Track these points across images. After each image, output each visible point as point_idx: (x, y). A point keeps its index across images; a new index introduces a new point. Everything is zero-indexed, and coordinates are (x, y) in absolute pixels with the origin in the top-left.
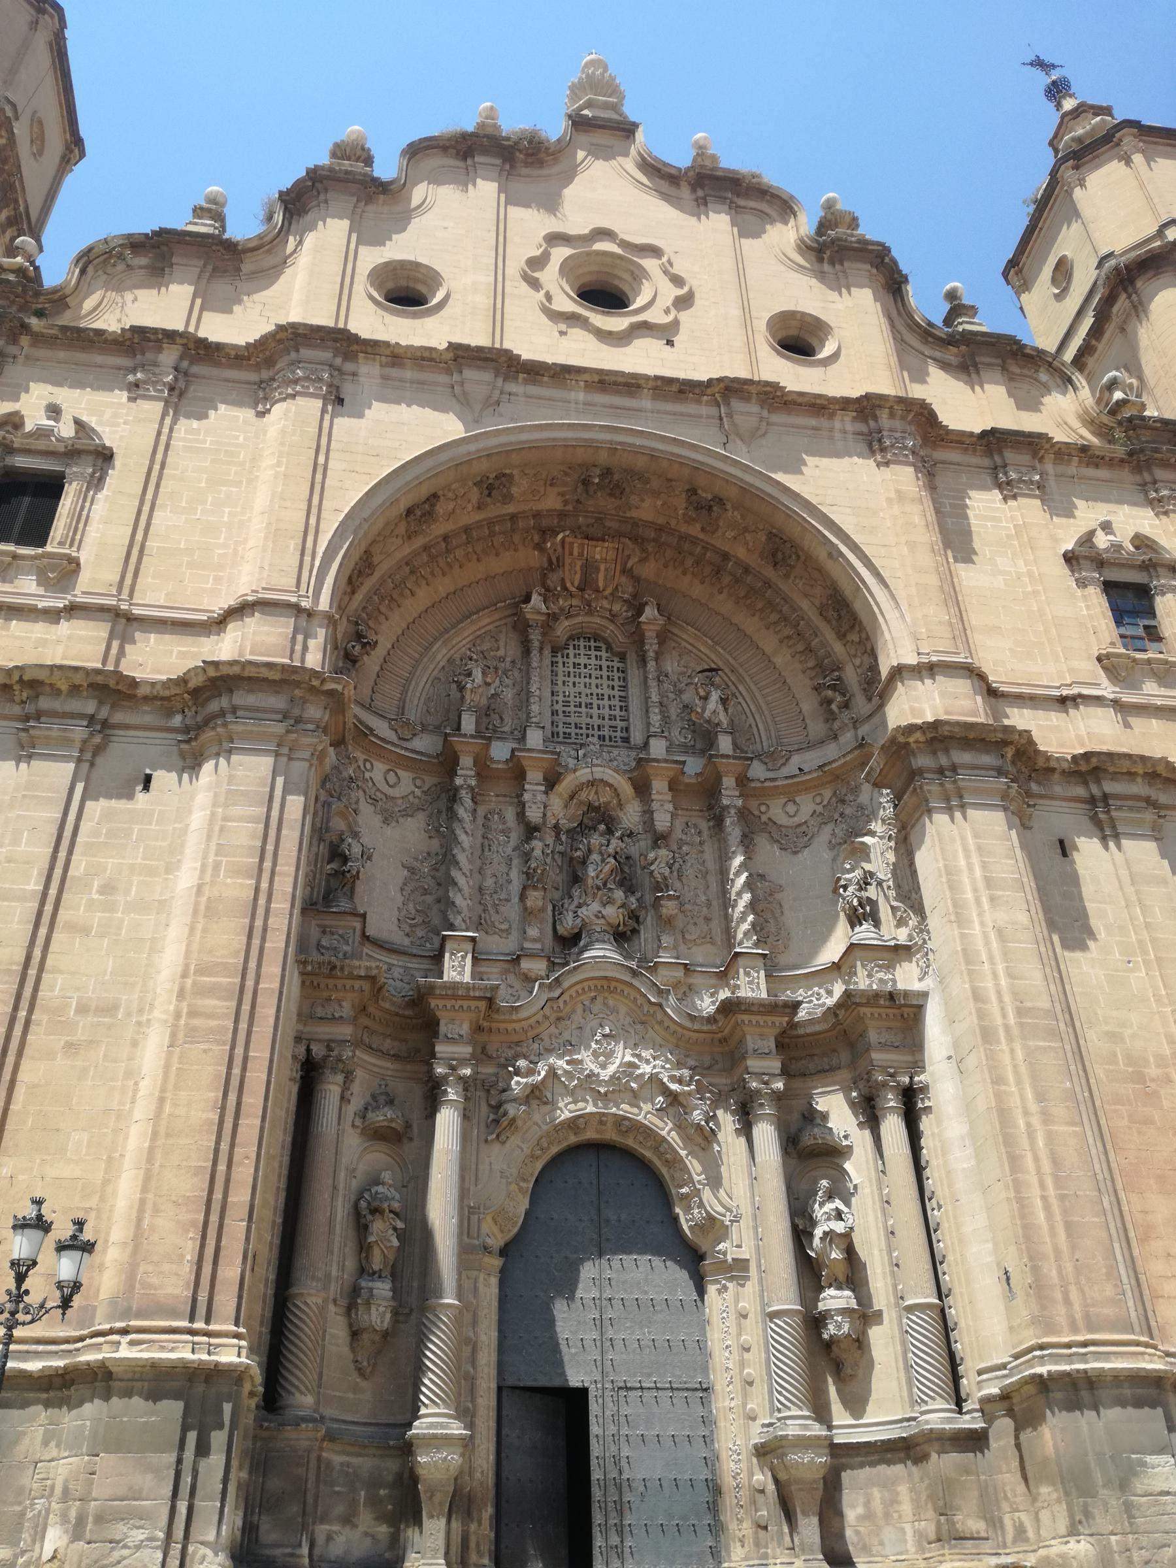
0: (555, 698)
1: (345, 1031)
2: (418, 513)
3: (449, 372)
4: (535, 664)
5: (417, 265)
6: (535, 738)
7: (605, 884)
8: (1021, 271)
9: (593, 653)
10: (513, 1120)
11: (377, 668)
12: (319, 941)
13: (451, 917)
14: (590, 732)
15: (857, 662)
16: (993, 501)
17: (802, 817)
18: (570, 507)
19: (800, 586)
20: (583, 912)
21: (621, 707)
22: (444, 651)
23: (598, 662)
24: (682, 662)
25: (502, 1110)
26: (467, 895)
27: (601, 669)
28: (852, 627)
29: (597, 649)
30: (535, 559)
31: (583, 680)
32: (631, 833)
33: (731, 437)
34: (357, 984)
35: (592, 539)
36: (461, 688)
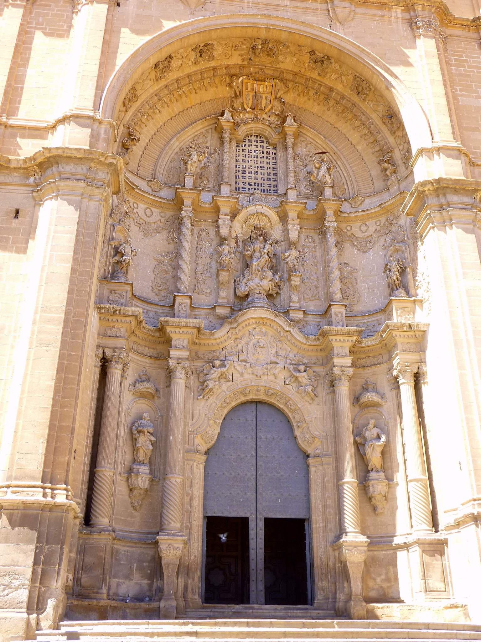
0: (238, 169)
1: (122, 343)
2: (162, 66)
4: (226, 150)
6: (225, 190)
7: (262, 269)
9: (259, 144)
10: (211, 389)
11: (141, 153)
12: (108, 297)
13: (179, 286)
14: (256, 187)
15: (401, 148)
17: (370, 233)
18: (246, 63)
19: (371, 106)
20: (250, 283)
21: (274, 174)
22: (177, 144)
23: (262, 149)
24: (307, 148)
25: (205, 384)
26: (187, 274)
27: (263, 153)
28: (399, 128)
29: (261, 142)
30: (228, 92)
31: (253, 159)
32: (277, 242)
33: (334, 21)
34: (128, 319)
35: (259, 81)
36: (186, 163)
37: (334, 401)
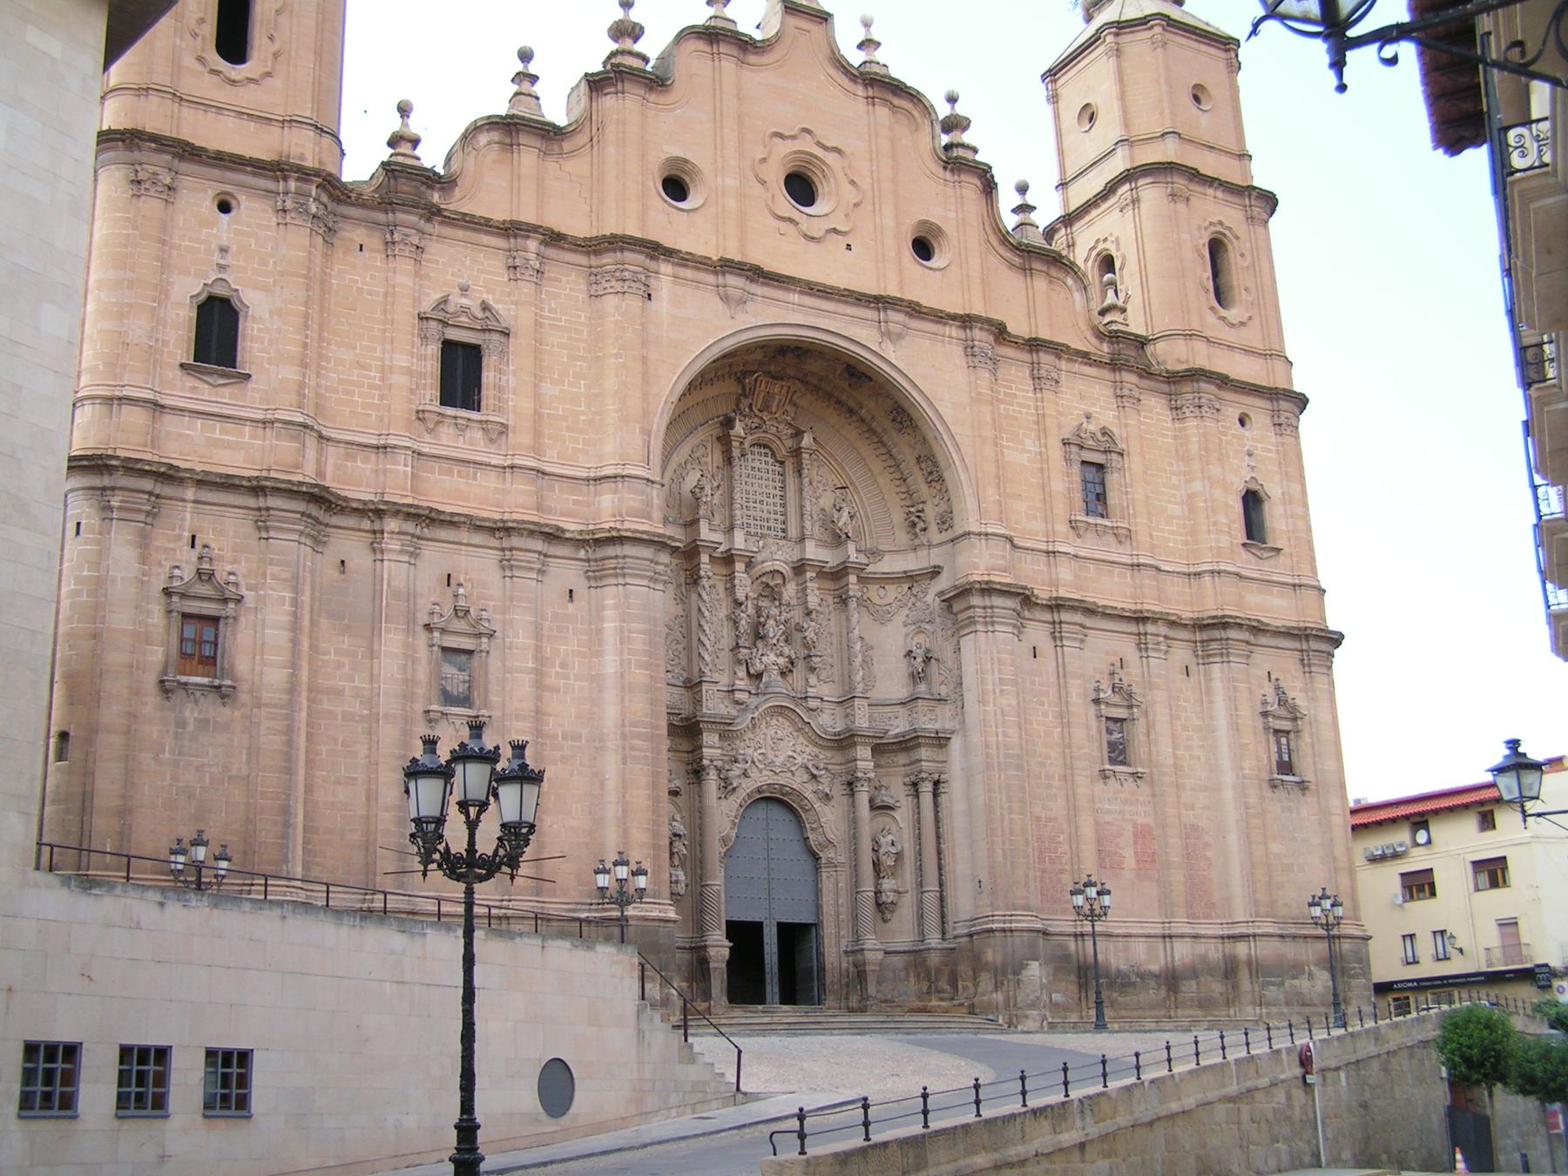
3: (716, 273)
5: (686, 161)
8: (1056, 81)
16: (1027, 391)
17: (890, 599)
20: (764, 659)
37: (853, 805)
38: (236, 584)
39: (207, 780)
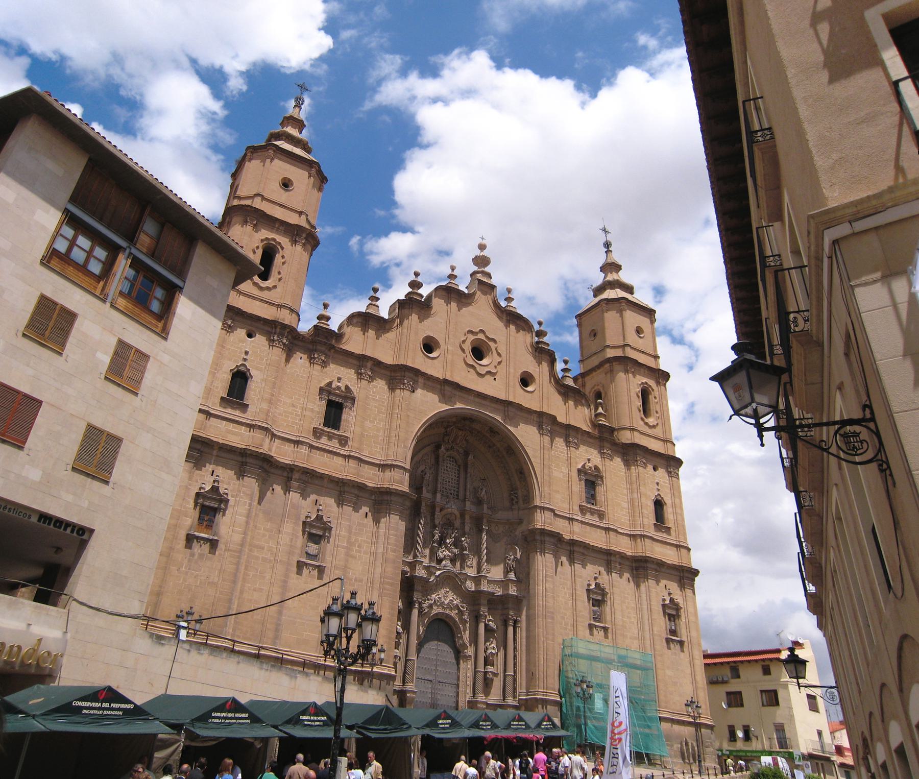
6: (439, 496)
38: (227, 494)
39: (198, 583)
